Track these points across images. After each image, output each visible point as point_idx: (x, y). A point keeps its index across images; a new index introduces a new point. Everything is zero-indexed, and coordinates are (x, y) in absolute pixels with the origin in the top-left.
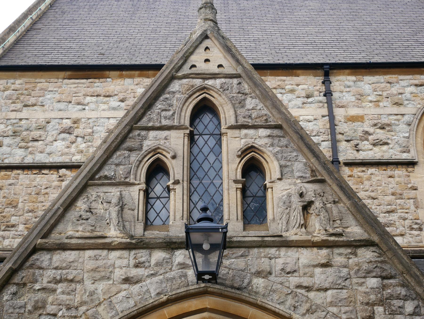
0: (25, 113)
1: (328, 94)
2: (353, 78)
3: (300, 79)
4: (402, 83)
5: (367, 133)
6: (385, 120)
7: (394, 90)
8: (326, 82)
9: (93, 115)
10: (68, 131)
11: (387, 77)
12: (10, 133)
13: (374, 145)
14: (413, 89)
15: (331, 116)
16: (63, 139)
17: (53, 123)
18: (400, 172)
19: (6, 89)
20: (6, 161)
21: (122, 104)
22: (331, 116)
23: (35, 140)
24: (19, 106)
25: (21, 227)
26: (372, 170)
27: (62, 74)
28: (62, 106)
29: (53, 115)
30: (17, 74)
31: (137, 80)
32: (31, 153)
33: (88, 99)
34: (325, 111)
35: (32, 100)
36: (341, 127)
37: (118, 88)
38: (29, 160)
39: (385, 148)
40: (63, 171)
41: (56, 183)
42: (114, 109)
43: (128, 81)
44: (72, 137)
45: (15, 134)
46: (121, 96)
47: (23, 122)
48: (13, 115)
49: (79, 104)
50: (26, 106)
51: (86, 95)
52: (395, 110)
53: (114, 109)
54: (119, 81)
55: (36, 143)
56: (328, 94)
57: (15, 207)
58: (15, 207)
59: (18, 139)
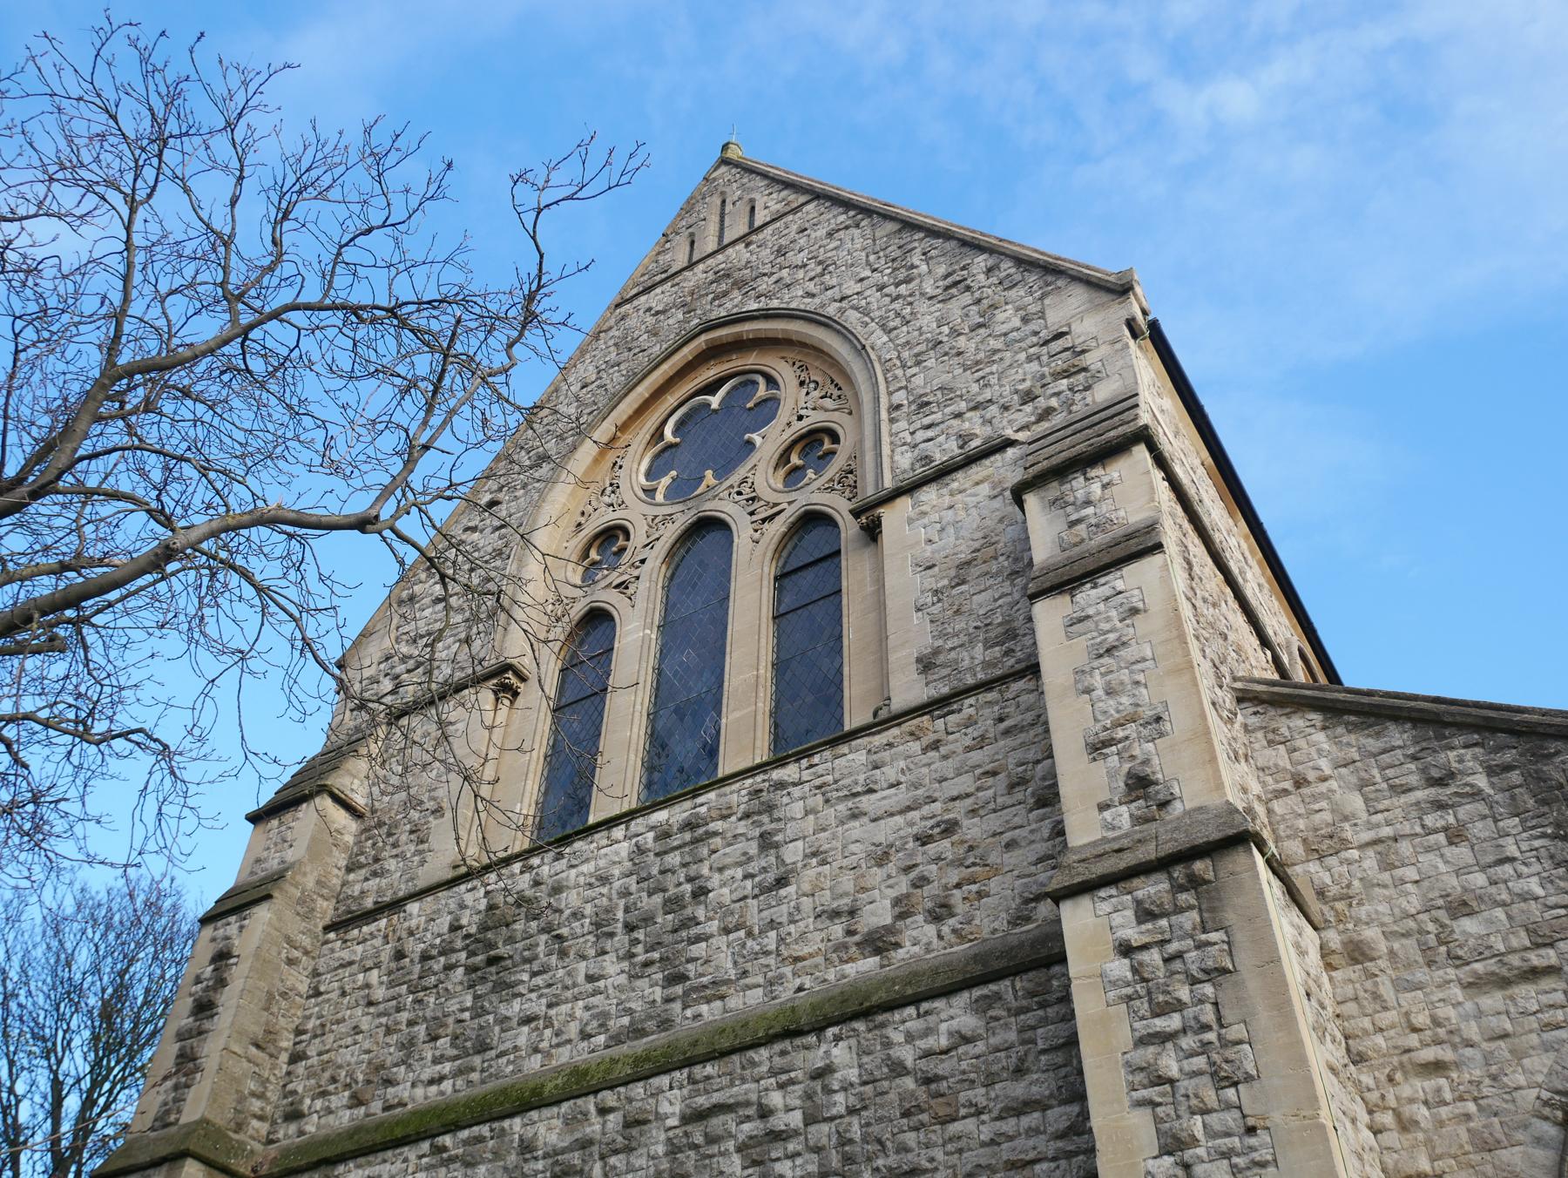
27: (1205, 454)
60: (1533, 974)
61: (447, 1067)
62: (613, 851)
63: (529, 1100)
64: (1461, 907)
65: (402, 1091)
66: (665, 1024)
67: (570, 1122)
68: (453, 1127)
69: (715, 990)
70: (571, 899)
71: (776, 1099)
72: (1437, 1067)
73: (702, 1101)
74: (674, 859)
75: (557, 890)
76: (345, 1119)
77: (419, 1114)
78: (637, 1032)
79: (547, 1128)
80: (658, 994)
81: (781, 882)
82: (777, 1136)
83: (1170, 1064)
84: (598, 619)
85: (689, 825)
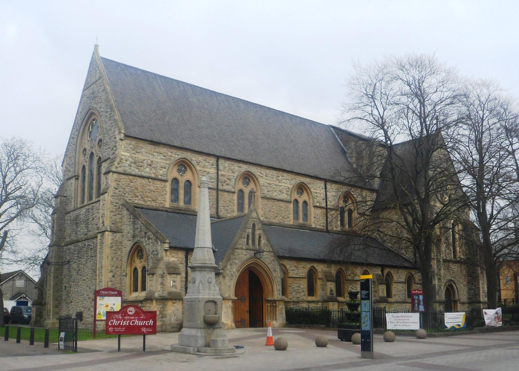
0: (137, 155)
1: (217, 165)
2: (224, 161)
3: (211, 158)
4: (235, 165)
5: (225, 181)
6: (230, 177)
7: (233, 167)
8: (217, 161)
9: (156, 160)
10: (150, 165)
11: (232, 162)
12: (133, 162)
13: (227, 185)
14: (237, 168)
15: (218, 173)
16: (149, 168)
17: (145, 161)
18: (231, 194)
19: (130, 144)
20: (133, 173)
21: (164, 158)
22: (218, 173)
23: (141, 167)
24: (135, 152)
25: (140, 197)
26: (225, 193)
27: (148, 142)
28: (147, 155)
29: (145, 158)
30: (134, 139)
31: (169, 149)
32: (140, 171)
33: (155, 154)
34: (216, 171)
35: (139, 151)
36: (220, 178)
37: (163, 151)
38: (139, 173)
39: (229, 186)
40: (150, 179)
41: (148, 183)
42: (162, 159)
43: (166, 149)
44: (151, 167)
45: (135, 163)
46: (165, 154)
47: (137, 159)
48: (133, 155)
49: (152, 155)
50: (136, 152)
51: (154, 152)
52: (232, 174)
53: (162, 159)
54: (163, 149)
55: (141, 168)
56: (217, 165)
57: (137, 190)
58: (137, 190)
59: (136, 165)
60: (130, 240)
61: (74, 235)
62: (84, 210)
63: (78, 241)
64: (128, 233)
65: (72, 237)
66: (87, 234)
67: (82, 244)
68: (74, 243)
69: (89, 231)
70: (81, 216)
71: (92, 245)
72: (125, 248)
73: (88, 244)
74: (87, 213)
75: (80, 215)
76: (69, 239)
77: (74, 241)
78: (85, 235)
79: (80, 244)
80: (86, 230)
81: (93, 220)
82: (92, 248)
83: (101, 251)
84: (84, 167)
85: (88, 209)
